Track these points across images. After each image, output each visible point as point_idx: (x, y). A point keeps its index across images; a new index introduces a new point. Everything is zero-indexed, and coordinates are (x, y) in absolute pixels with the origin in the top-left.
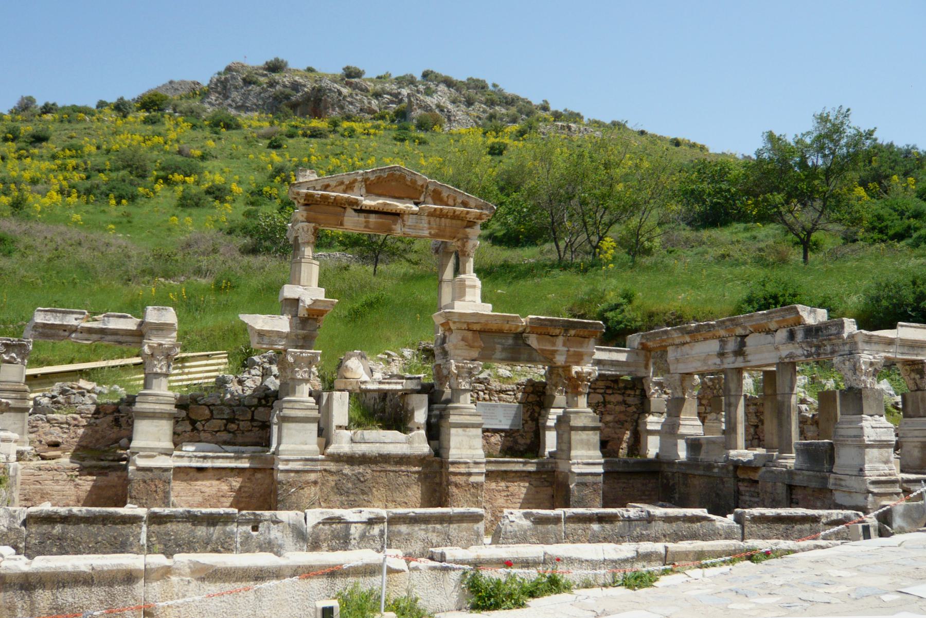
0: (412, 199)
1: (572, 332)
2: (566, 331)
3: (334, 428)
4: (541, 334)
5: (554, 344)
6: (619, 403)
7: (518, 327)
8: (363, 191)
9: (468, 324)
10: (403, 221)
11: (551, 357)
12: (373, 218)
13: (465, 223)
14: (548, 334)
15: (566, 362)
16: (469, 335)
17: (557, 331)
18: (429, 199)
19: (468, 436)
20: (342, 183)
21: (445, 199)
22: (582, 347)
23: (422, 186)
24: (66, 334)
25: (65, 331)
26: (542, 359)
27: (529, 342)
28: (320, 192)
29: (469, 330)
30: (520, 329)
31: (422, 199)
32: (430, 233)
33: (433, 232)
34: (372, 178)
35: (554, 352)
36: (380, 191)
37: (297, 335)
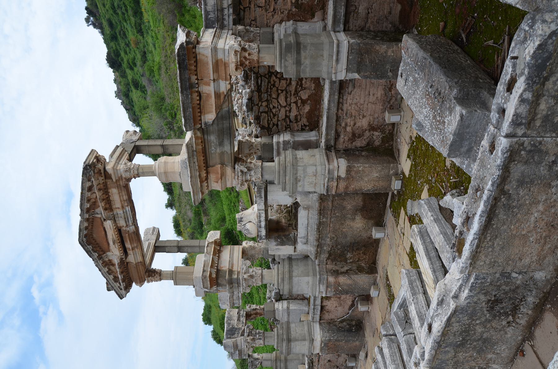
0: (102, 223)
1: (194, 78)
2: (191, 86)
3: (296, 253)
4: (200, 112)
7: (196, 138)
8: (108, 253)
9: (201, 182)
10: (123, 226)
11: (222, 97)
12: (128, 245)
13: (109, 182)
14: (199, 104)
15: (226, 80)
16: (212, 177)
17: (195, 95)
18: (97, 210)
19: (305, 177)
20: (109, 269)
21: (93, 200)
22: (207, 63)
23: (87, 220)
26: (227, 103)
27: (211, 121)
28: (122, 284)
29: (207, 179)
30: (199, 134)
31: (99, 216)
32: (128, 206)
33: (126, 204)
34: (96, 255)
35: (217, 95)
36: (105, 244)
37: (231, 288)
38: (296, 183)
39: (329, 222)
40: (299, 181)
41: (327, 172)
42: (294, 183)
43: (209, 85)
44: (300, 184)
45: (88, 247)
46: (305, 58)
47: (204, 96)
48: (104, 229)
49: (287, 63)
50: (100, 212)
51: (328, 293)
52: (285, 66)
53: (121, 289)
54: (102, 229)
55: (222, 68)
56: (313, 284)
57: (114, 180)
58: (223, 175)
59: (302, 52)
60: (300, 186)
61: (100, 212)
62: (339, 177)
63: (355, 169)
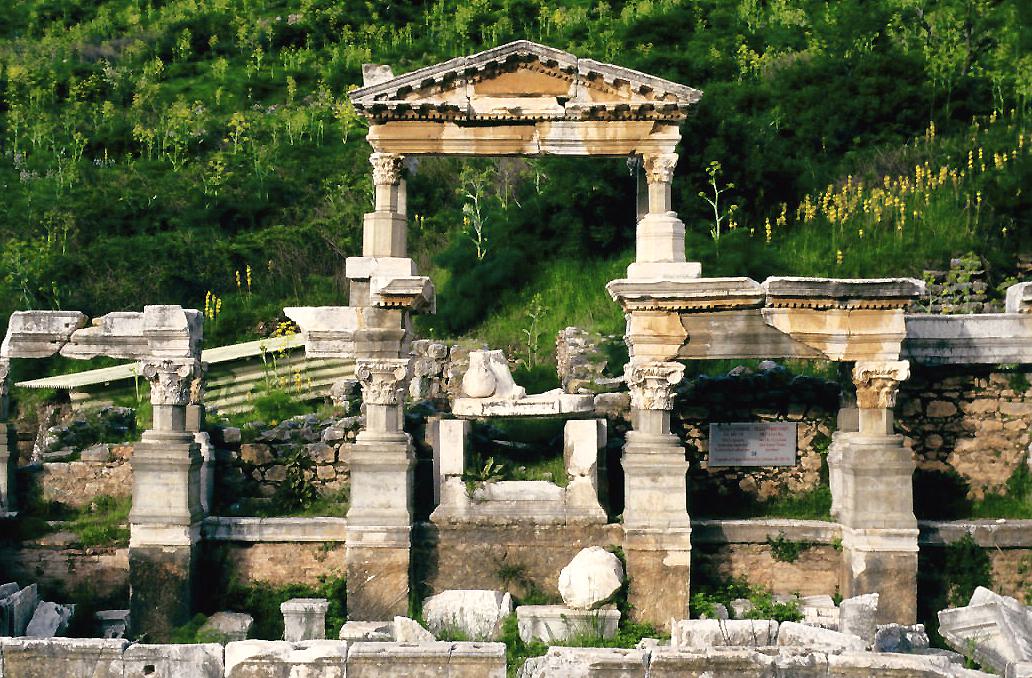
0: (552, 95)
5: (822, 323)
6: (991, 415)
22: (875, 326)
24: (56, 346)
25: (55, 342)
28: (396, 103)
35: (823, 339)
37: (370, 337)
38: (648, 475)
39: (532, 543)
40: (653, 480)
41: (678, 530)
42: (650, 471)
43: (841, 327)
44: (647, 481)
45: (505, 57)
46: (888, 484)
47: (820, 315)
48: (538, 95)
49: (879, 454)
50: (585, 98)
51: (357, 551)
52: (875, 451)
53: (376, 99)
54: (538, 91)
55: (865, 348)
56: (383, 516)
57: (656, 136)
58: (663, 339)
59: (900, 477)
60: (642, 482)
61: (585, 98)
62: (664, 553)
63: (680, 582)
